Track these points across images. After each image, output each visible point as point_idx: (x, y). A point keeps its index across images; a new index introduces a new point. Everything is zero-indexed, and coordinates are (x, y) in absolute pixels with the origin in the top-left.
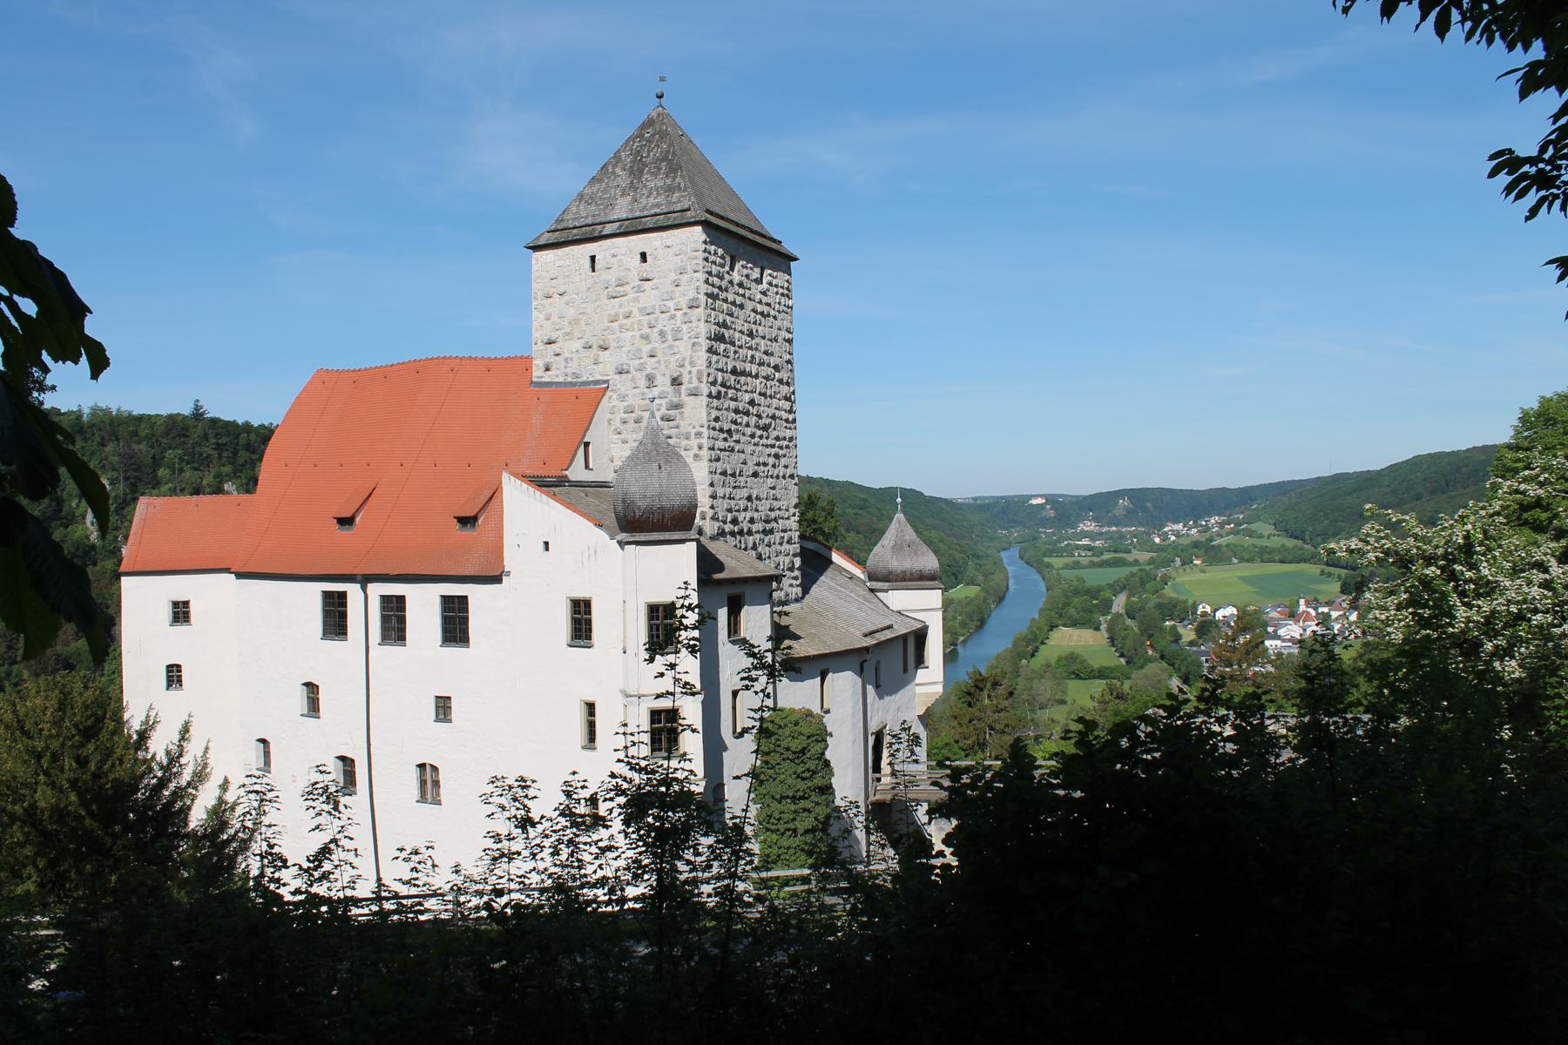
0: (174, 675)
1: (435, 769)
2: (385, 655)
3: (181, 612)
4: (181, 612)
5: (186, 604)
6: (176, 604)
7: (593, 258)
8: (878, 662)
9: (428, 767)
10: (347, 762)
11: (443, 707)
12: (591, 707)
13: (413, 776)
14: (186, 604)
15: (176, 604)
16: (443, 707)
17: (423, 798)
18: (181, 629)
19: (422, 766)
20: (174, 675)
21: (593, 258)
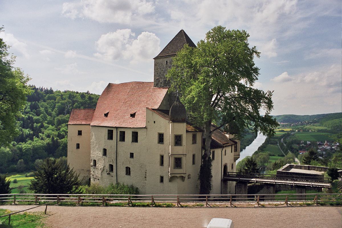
0: (78, 146)
1: (129, 168)
2: (120, 143)
3: (80, 133)
4: (80, 133)
5: (81, 131)
6: (79, 131)
7: (167, 61)
8: (226, 150)
9: (128, 169)
10: (111, 166)
11: (132, 155)
12: (162, 157)
13: (125, 170)
14: (81, 131)
15: (79, 131)
16: (132, 155)
17: (127, 174)
18: (80, 136)
19: (127, 168)
20: (78, 146)
21: (167, 61)
